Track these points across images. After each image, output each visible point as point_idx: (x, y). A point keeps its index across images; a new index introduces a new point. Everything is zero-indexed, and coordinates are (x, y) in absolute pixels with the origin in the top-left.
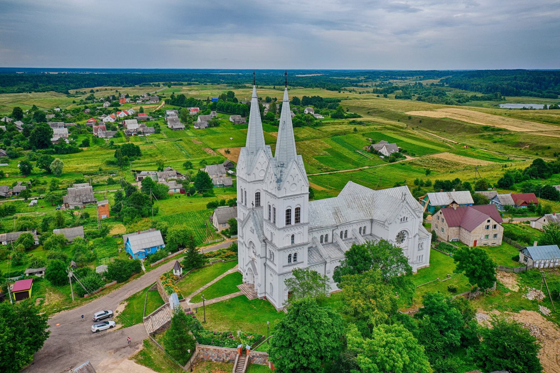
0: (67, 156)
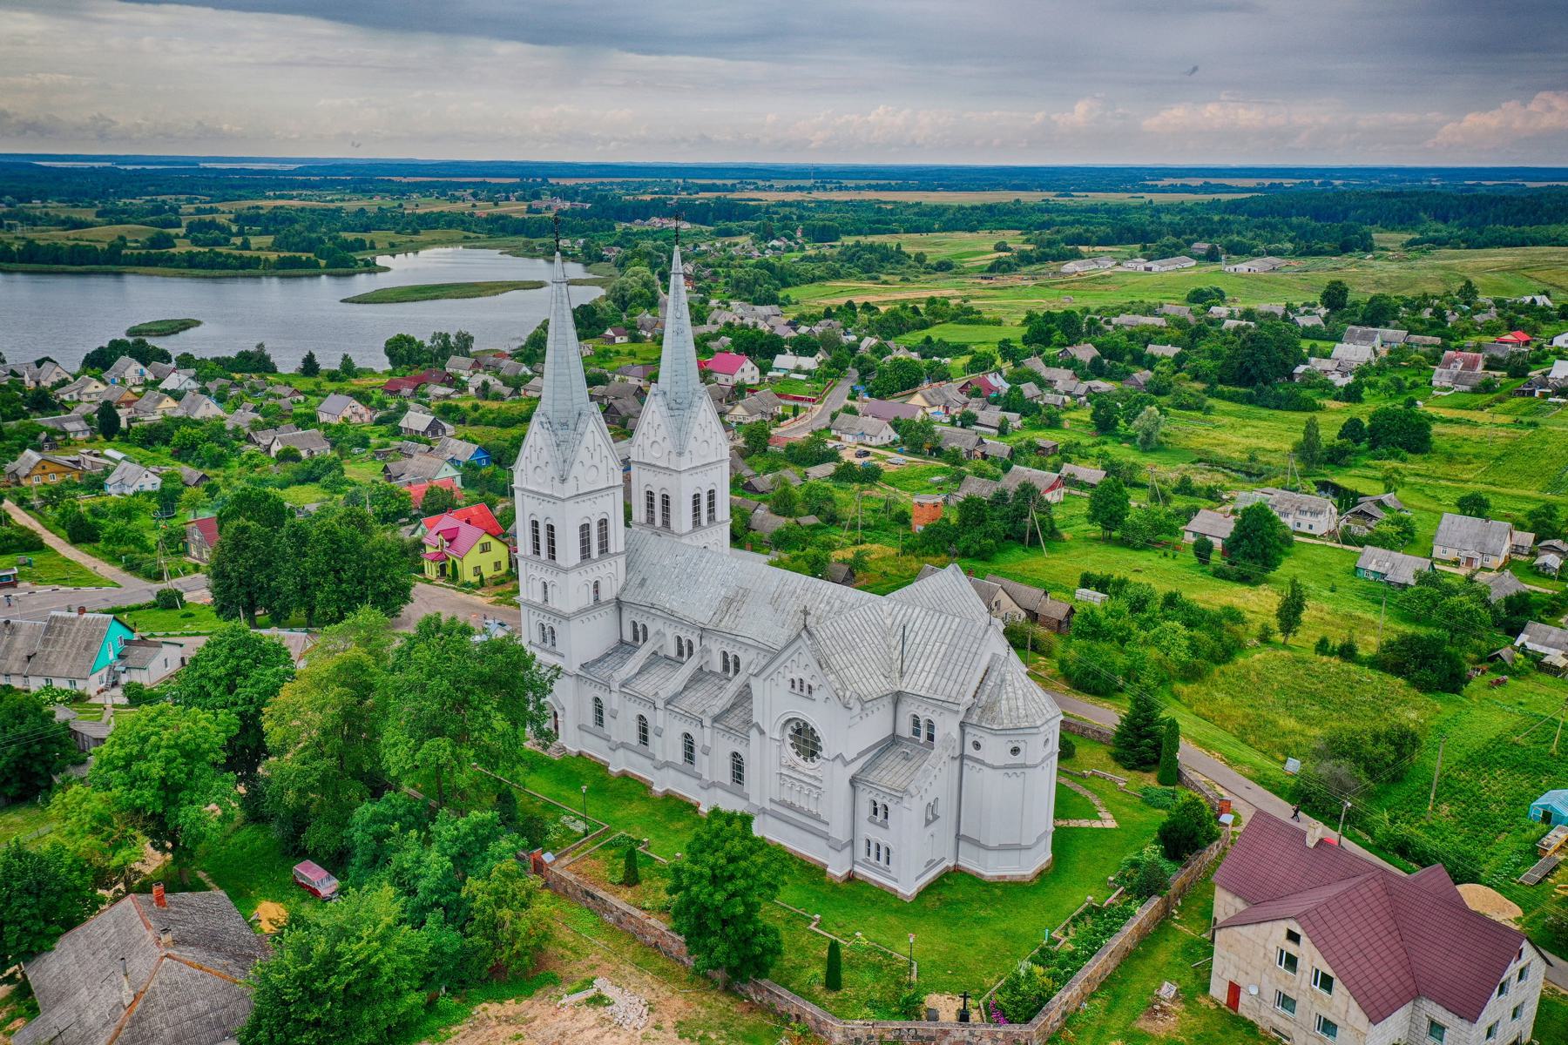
0: (1265, 412)
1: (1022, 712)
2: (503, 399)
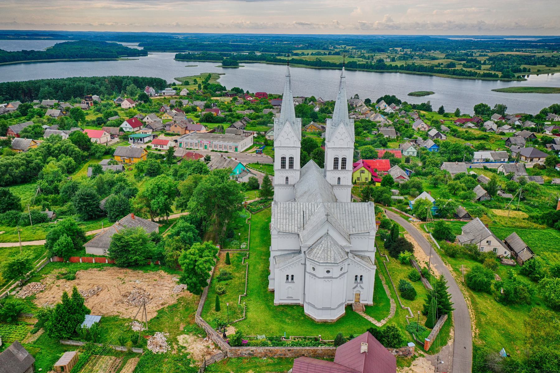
1: (319, 255)
2: (486, 131)
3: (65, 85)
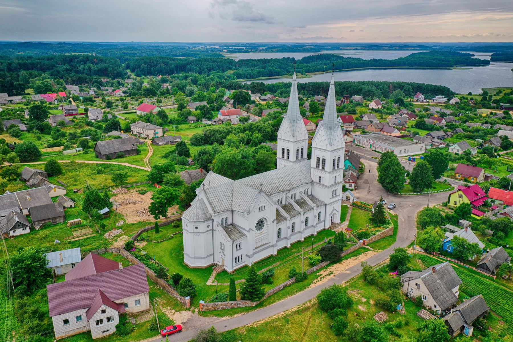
3: (351, 86)
